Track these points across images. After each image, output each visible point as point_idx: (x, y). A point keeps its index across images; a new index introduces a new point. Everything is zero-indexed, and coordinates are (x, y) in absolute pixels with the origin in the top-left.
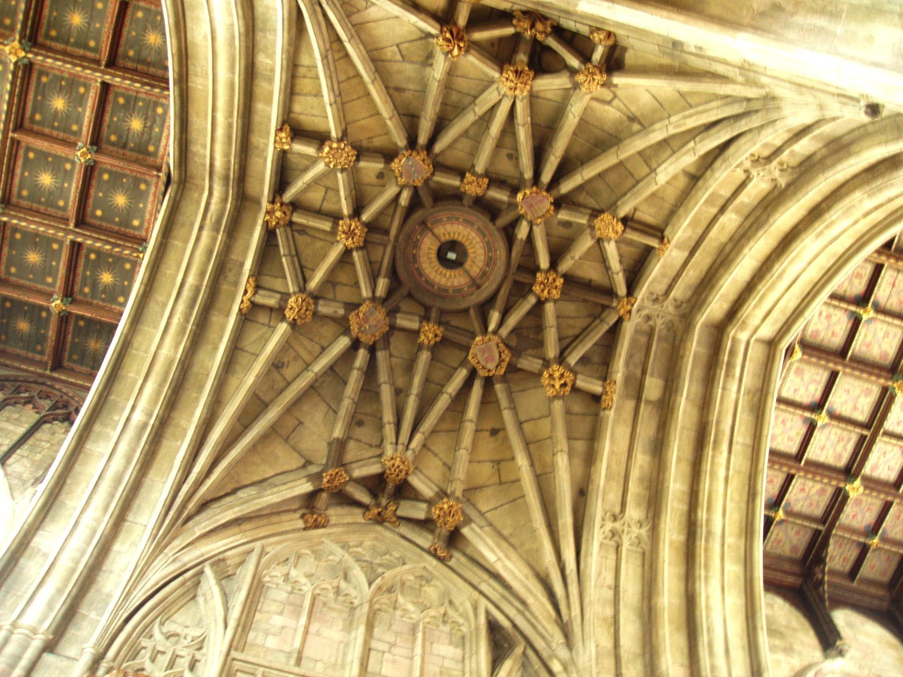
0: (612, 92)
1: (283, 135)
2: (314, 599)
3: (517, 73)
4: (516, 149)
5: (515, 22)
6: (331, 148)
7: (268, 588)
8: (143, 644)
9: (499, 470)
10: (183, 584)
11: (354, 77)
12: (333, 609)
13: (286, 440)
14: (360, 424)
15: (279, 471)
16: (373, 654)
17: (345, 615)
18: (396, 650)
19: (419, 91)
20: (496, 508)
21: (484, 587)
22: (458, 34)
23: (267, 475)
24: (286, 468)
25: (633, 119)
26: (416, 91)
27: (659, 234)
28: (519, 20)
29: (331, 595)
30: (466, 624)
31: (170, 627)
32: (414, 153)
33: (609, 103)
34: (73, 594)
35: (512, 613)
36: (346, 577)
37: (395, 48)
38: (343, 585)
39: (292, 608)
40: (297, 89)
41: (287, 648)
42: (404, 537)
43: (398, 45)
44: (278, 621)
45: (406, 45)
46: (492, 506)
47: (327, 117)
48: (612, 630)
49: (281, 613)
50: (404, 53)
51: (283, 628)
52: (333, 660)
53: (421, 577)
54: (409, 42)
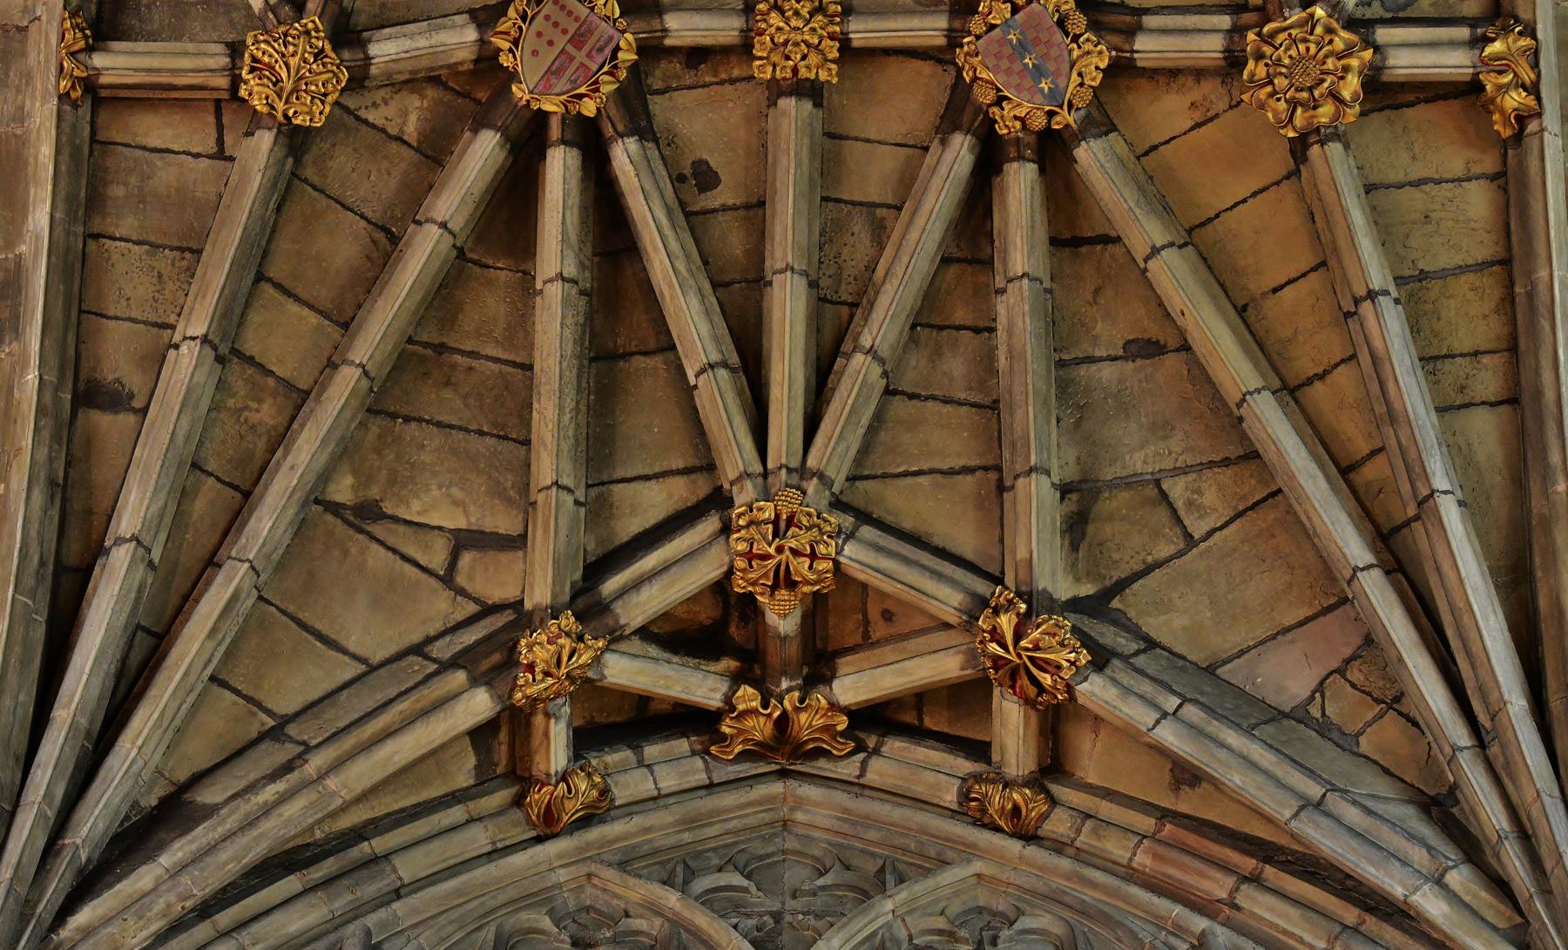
0: (461, 592)
1: (1515, 99)
3: (784, 580)
4: (693, 220)
5: (842, 723)
6: (1335, 96)
11: (1309, 382)
19: (1079, 361)
22: (1014, 674)
25: (365, 514)
26: (1091, 360)
27: (104, 93)
28: (828, 729)
32: (1039, 122)
33: (464, 541)
37: (1198, 528)
40: (1490, 283)
43: (1190, 541)
45: (1164, 551)
47: (1369, 189)
50: (1163, 514)
54: (1158, 565)
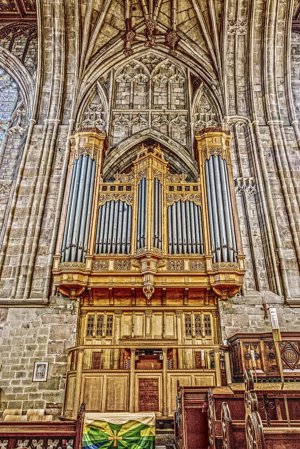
8: (86, 114)
9: (188, 13)
12: (140, 85)
14: (134, 9)
16: (155, 97)
17: (144, 86)
21: (188, 63)
30: (184, 79)
31: (93, 106)
34: (61, 105)
35: (199, 71)
38: (142, 75)
41: (128, 103)
42: (159, 50)
44: (124, 94)
49: (124, 91)
52: (143, 103)
53: (168, 64)
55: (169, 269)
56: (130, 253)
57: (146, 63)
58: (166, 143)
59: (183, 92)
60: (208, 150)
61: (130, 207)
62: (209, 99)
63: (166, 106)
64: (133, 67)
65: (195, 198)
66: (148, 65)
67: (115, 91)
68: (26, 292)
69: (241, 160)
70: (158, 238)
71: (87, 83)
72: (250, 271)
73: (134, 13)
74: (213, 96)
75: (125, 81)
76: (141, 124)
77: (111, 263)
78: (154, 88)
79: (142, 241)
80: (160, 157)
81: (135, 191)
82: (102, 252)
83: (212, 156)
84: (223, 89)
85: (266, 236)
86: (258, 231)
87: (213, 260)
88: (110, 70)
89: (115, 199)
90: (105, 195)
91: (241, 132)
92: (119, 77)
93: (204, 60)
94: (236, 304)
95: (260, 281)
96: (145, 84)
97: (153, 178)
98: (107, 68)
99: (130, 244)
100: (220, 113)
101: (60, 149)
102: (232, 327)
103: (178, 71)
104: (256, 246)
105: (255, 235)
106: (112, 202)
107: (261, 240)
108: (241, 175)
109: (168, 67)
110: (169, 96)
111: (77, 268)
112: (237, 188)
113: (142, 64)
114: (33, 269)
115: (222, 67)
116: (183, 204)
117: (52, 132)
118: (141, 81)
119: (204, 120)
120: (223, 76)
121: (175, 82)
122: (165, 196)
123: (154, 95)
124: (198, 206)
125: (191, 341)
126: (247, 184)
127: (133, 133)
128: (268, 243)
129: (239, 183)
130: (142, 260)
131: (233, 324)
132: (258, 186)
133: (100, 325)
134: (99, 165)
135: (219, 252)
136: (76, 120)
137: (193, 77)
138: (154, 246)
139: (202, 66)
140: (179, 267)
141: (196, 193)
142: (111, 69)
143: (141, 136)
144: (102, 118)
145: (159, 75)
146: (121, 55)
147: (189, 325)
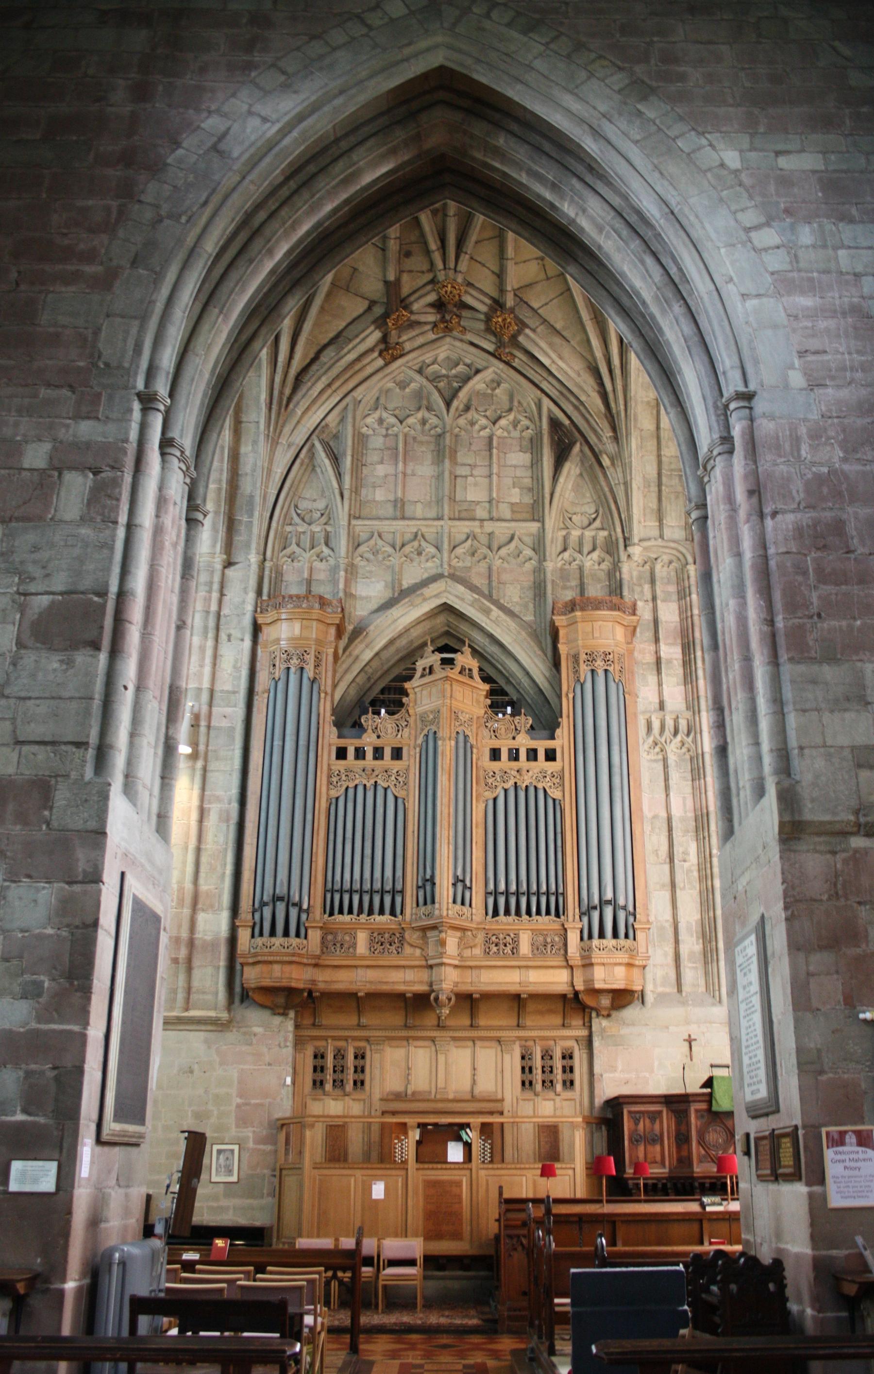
2: (406, 436)
7: (368, 436)
10: (302, 464)
12: (421, 443)
13: (347, 290)
14: (408, 254)
15: (349, 320)
16: (459, 480)
18: (475, 472)
20: (546, 304)
21: (544, 385)
23: (341, 328)
24: (355, 314)
29: (418, 427)
30: (532, 426)
35: (569, 409)
36: (429, 409)
39: (389, 452)
42: (472, 344)
44: (381, 470)
46: (543, 302)
48: (655, 412)
49: (382, 462)
51: (386, 476)
52: (428, 498)
53: (493, 381)
55: (487, 953)
56: (402, 913)
57: (434, 379)
58: (484, 618)
59: (528, 464)
60: (583, 657)
61: (400, 801)
62: (594, 488)
63: (487, 505)
64: (404, 388)
65: (548, 779)
66: (441, 385)
67: (358, 464)
68: (181, 996)
69: (663, 666)
70: (463, 881)
71: (289, 446)
72: (667, 949)
73: (409, 263)
74: (603, 484)
75: (384, 432)
76: (423, 558)
77: (362, 938)
78: (456, 452)
79: (428, 888)
80: (471, 677)
81: (411, 758)
82: (341, 912)
83: (593, 671)
84: (626, 468)
85: (708, 865)
86: (693, 848)
87: (581, 932)
88: (344, 403)
89: (365, 782)
90: (342, 771)
91: (669, 582)
92: (369, 420)
93: (582, 384)
94: (628, 1025)
95: (687, 970)
96: (433, 439)
97: (454, 735)
98: (338, 398)
99: (402, 892)
100: (620, 535)
101: (229, 637)
102: (617, 1075)
103: (519, 402)
104: (684, 888)
105: (685, 861)
106: (360, 790)
107: (696, 874)
108: (662, 706)
109: (494, 389)
110: (495, 477)
111: (290, 950)
112: (651, 739)
113: (425, 382)
114: (191, 943)
115: (626, 410)
116: (522, 795)
117: (210, 592)
118: (423, 431)
119: (580, 552)
120: (628, 434)
121: (509, 433)
122: (482, 773)
123: (458, 473)
124: (554, 800)
125: (531, 1103)
126: (676, 732)
127: (405, 585)
128: (709, 883)
129: (656, 725)
130: (430, 934)
131: (620, 1068)
132: (698, 736)
133: (340, 1069)
134: (326, 693)
135: (596, 915)
136: (265, 554)
137: (555, 424)
138: (454, 902)
139: (577, 398)
140: (509, 947)
141: (551, 767)
142: (348, 400)
143: (425, 600)
144: (327, 544)
145: (469, 415)
146: (373, 360)
147: (527, 1069)
